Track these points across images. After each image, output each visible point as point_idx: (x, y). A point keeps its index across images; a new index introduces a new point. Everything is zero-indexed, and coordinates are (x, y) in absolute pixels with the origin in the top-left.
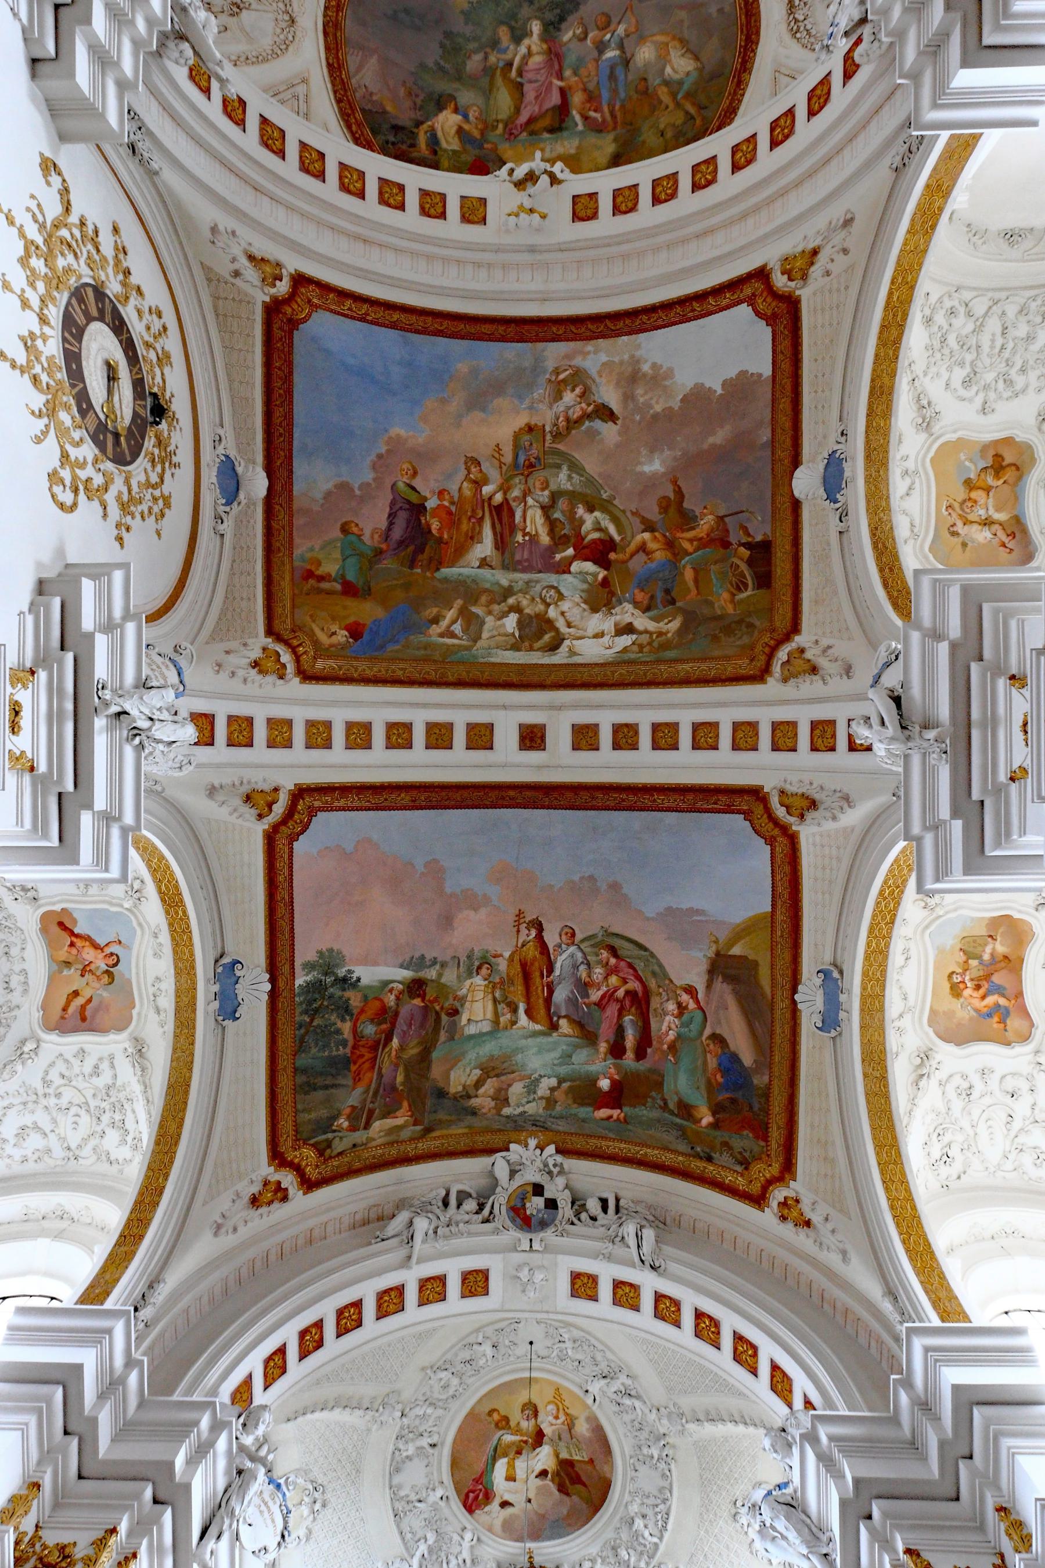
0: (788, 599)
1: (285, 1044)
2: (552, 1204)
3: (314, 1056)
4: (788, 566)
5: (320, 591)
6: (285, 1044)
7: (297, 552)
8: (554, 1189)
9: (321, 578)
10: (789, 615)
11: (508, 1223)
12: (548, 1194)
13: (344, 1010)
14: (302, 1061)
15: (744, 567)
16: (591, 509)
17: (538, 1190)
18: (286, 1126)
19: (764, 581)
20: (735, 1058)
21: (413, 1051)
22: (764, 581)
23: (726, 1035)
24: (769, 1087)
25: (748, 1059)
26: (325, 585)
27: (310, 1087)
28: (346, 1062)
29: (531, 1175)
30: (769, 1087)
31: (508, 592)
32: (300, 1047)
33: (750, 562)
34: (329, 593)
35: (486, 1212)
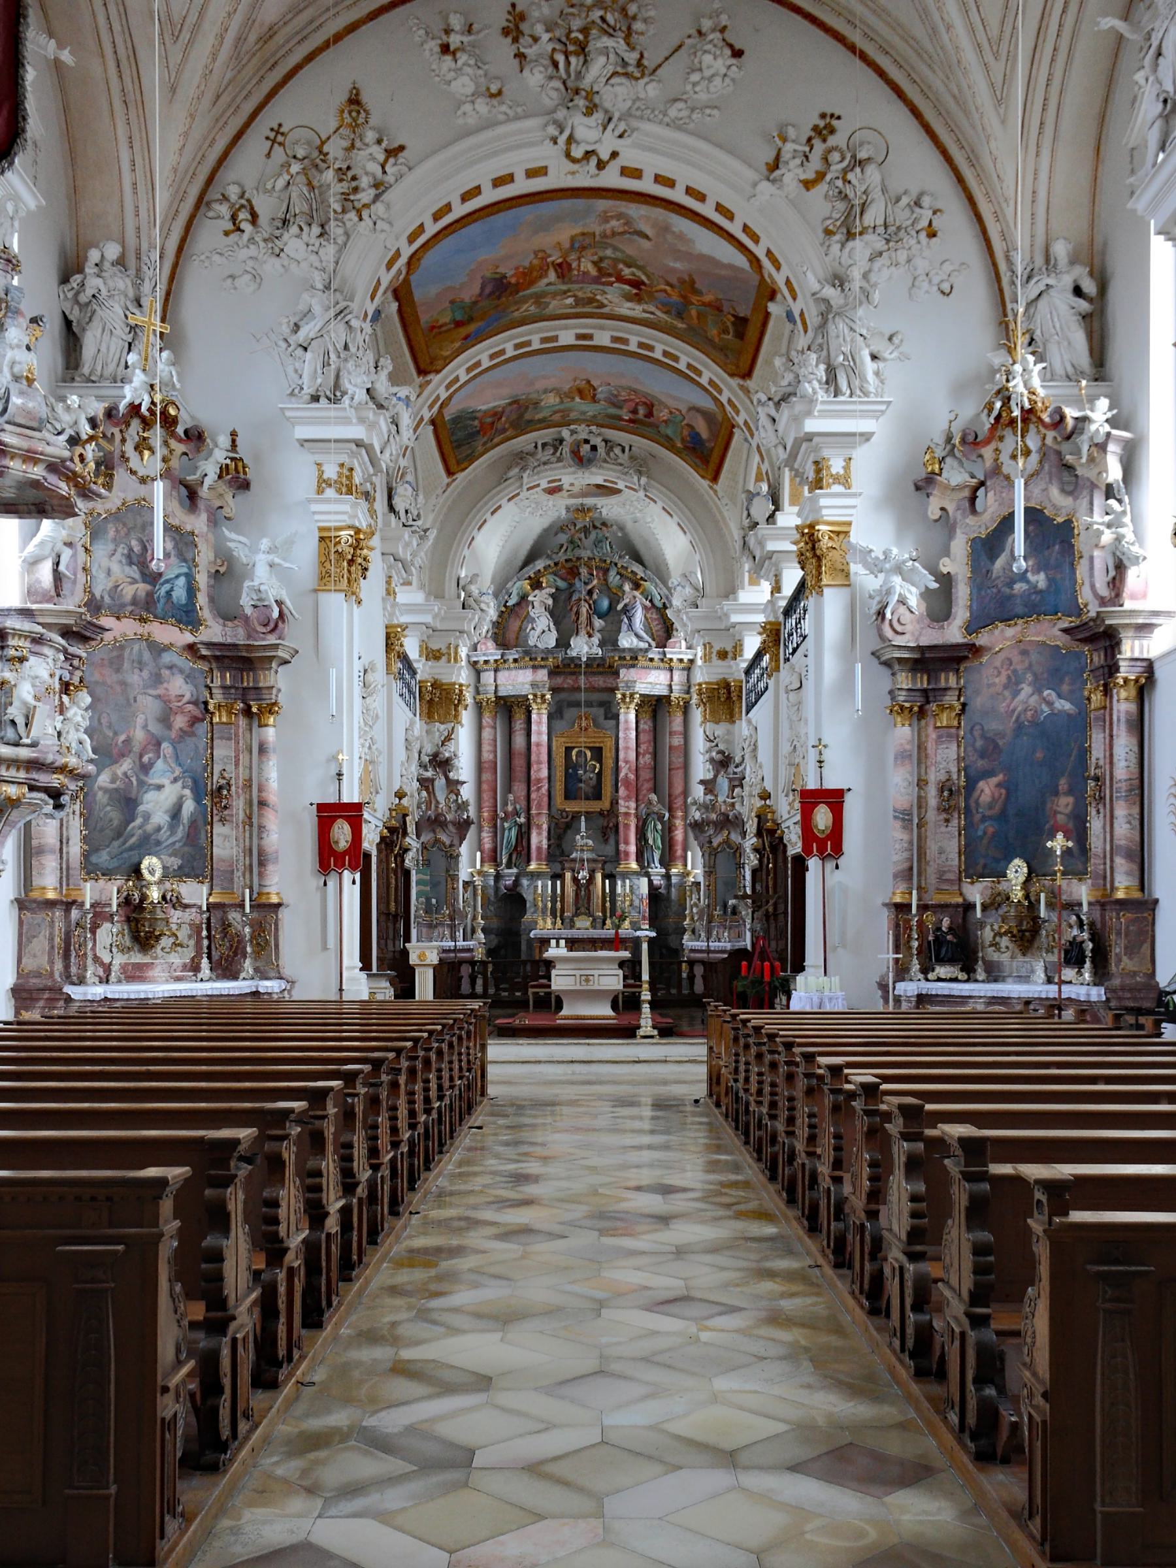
0: (751, 350)
1: (444, 436)
2: (594, 448)
3: (460, 435)
4: (757, 334)
5: (440, 333)
6: (444, 436)
7: (422, 321)
8: (597, 441)
9: (441, 326)
10: (749, 362)
11: (571, 462)
12: (592, 443)
13: (475, 418)
14: (455, 438)
15: (729, 324)
16: (629, 266)
17: (587, 441)
18: (452, 462)
19: (740, 335)
20: (698, 434)
21: (514, 416)
22: (740, 335)
23: (694, 424)
24: (713, 448)
25: (705, 435)
26: (444, 329)
27: (459, 446)
28: (478, 432)
29: (584, 436)
30: (713, 448)
31: (569, 291)
32: (453, 434)
33: (733, 324)
34: (450, 330)
35: (558, 454)
